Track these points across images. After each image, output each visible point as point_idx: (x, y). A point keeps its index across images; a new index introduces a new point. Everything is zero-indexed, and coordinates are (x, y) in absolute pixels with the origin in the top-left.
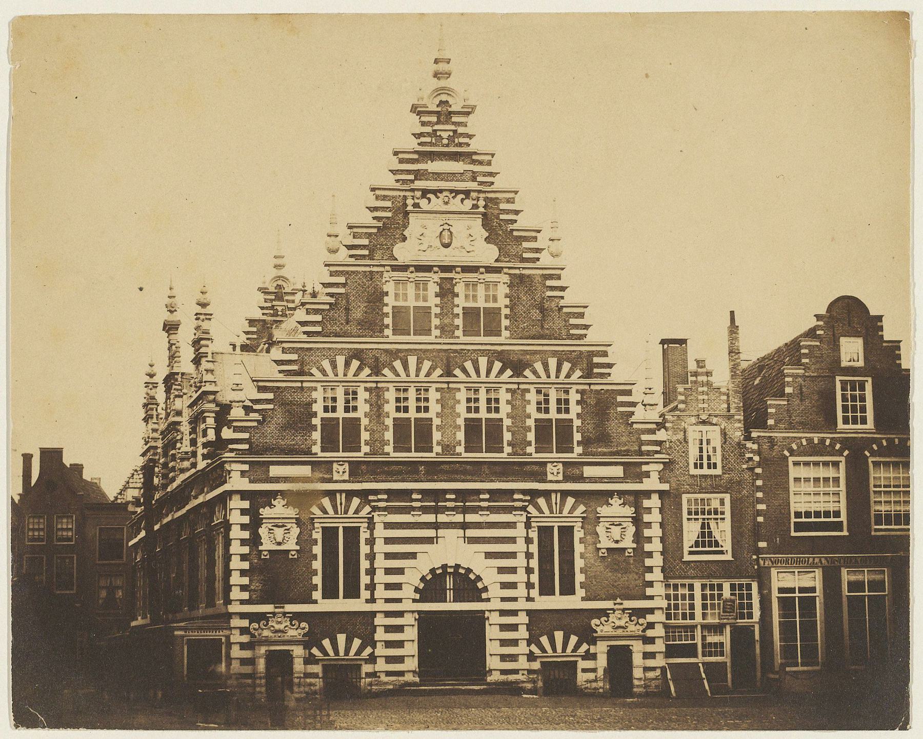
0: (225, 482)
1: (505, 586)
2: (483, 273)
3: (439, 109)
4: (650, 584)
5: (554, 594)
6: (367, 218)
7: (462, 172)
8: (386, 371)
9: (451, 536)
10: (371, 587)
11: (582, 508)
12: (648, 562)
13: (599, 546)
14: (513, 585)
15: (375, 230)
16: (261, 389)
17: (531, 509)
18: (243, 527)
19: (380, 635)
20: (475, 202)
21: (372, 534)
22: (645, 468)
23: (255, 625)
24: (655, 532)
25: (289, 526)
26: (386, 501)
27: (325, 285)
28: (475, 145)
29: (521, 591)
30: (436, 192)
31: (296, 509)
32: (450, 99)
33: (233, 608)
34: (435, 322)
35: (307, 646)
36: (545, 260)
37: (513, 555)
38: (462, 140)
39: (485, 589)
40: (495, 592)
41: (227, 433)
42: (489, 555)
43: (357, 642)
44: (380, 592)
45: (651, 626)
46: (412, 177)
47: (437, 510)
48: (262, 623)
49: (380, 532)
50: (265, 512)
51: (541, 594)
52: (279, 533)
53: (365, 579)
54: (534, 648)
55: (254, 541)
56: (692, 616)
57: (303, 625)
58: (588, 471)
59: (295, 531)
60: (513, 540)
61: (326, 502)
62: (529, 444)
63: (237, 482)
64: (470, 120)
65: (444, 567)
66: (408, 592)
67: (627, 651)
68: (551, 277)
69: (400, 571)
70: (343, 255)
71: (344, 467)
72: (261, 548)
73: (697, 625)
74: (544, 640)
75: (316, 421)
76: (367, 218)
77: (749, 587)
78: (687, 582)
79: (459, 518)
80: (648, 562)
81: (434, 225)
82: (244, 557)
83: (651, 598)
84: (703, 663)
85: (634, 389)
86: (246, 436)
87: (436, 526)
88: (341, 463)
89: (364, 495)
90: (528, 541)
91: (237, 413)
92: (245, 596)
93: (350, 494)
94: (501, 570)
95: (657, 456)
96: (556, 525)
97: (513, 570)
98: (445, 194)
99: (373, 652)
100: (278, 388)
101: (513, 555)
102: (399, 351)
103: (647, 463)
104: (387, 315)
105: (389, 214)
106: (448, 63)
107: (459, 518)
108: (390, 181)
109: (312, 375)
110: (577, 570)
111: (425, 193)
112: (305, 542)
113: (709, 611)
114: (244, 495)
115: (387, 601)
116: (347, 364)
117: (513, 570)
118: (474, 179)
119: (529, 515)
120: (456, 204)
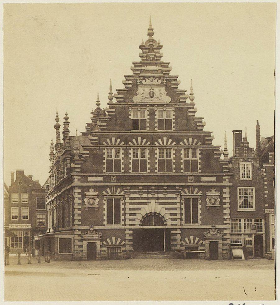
0: (73, 183)
1: (172, 220)
2: (165, 107)
3: (149, 47)
4: (225, 220)
5: (190, 223)
6: (123, 87)
7: (158, 70)
8: (130, 143)
9: (153, 202)
10: (125, 220)
11: (201, 192)
12: (225, 211)
13: (207, 206)
14: (175, 220)
15: (126, 92)
16: (85, 150)
17: (182, 192)
18: (79, 199)
20: (162, 81)
21: (125, 201)
22: (224, 178)
23: (83, 233)
24: (227, 200)
25: (95, 198)
26: (130, 189)
27: (108, 112)
29: (178, 222)
30: (148, 78)
31: (98, 193)
33: (74, 228)
34: (148, 125)
35: (102, 241)
36: (188, 101)
37: (176, 209)
38: (157, 58)
39: (165, 221)
40: (169, 222)
41: (73, 165)
42: (167, 209)
43: (119, 240)
44: (128, 222)
45: (225, 234)
47: (148, 193)
49: (128, 200)
50: (87, 193)
51: (185, 223)
53: (122, 217)
54: (183, 242)
56: (241, 231)
57: (100, 233)
58: (203, 179)
59: (97, 200)
60: (175, 203)
61: (108, 190)
62: (182, 169)
63: (76, 182)
64: (161, 51)
65: (151, 213)
66: (137, 222)
67: (217, 243)
68: (190, 108)
69: (135, 214)
70: (114, 101)
72: (85, 206)
73: (242, 234)
74: (187, 239)
75: (105, 161)
76: (123, 87)
77: (261, 220)
78: (239, 219)
79: (156, 196)
80: (225, 211)
83: (226, 224)
85: (220, 149)
87: (148, 198)
89: (123, 186)
90: (181, 204)
91: (76, 158)
92: (80, 223)
93: (117, 187)
94: (171, 214)
95: (228, 173)
96: (191, 198)
97: (175, 214)
98: (151, 78)
99: (125, 243)
100: (91, 149)
101: (176, 209)
102: (135, 135)
103: (225, 176)
105: (131, 86)
106: (153, 30)
107: (156, 196)
108: (131, 73)
109: (103, 144)
110: (199, 214)
111: (144, 78)
112: (101, 204)
113: (247, 229)
114: (79, 187)
115: (130, 225)
116: (116, 141)
117: (175, 214)
118: (162, 73)
119: (182, 195)
120: (155, 82)
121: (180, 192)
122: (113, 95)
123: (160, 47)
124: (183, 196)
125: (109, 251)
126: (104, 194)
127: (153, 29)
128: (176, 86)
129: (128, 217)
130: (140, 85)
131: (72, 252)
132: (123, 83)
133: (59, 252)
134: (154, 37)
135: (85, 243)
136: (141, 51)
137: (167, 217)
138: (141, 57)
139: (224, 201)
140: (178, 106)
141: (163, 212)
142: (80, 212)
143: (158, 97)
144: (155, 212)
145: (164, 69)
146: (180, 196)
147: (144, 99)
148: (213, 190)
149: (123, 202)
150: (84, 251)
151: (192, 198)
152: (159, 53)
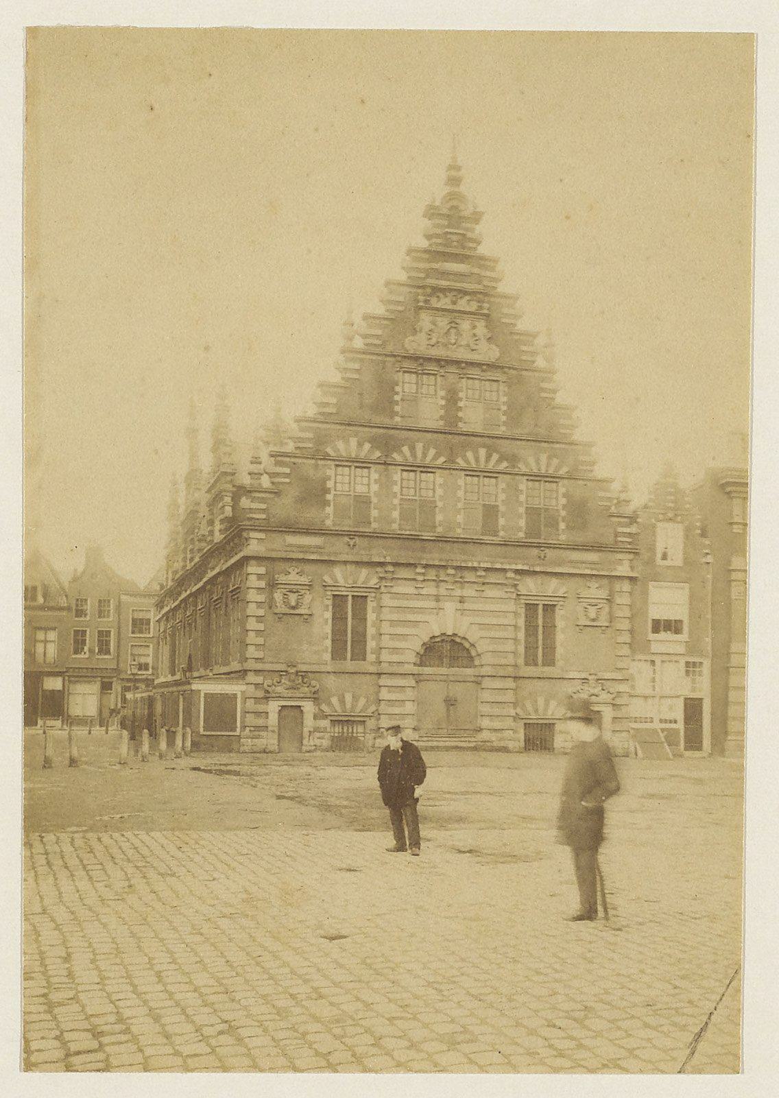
6: (380, 310)
16: (277, 463)
22: (620, 556)
28: (482, 250)
32: (462, 207)
36: (540, 363)
38: (471, 245)
40: (487, 659)
46: (422, 275)
49: (387, 600)
52: (293, 599)
53: (371, 644)
54: (519, 710)
55: (271, 604)
64: (478, 228)
66: (412, 657)
69: (404, 637)
71: (354, 540)
75: (329, 497)
79: (458, 592)
81: (443, 322)
82: (260, 619)
84: (663, 730)
86: (264, 506)
88: (352, 537)
92: (260, 655)
104: (397, 403)
107: (458, 592)
111: (436, 290)
119: (519, 593)
120: (463, 304)
121: (515, 586)
122: (355, 327)
123: (477, 217)
124: (521, 597)
125: (337, 731)
127: (459, 168)
129: (386, 641)
130: (421, 308)
131: (238, 730)
132: (382, 301)
133: (201, 730)
134: (463, 189)
135: (273, 707)
136: (427, 222)
137: (482, 646)
138: (428, 237)
140: (514, 372)
141: (473, 635)
142: (261, 627)
143: (468, 345)
144: (454, 634)
145: (483, 273)
146: (514, 596)
147: (433, 346)
148: (594, 584)
149: (375, 604)
151: (543, 603)
152: (472, 230)
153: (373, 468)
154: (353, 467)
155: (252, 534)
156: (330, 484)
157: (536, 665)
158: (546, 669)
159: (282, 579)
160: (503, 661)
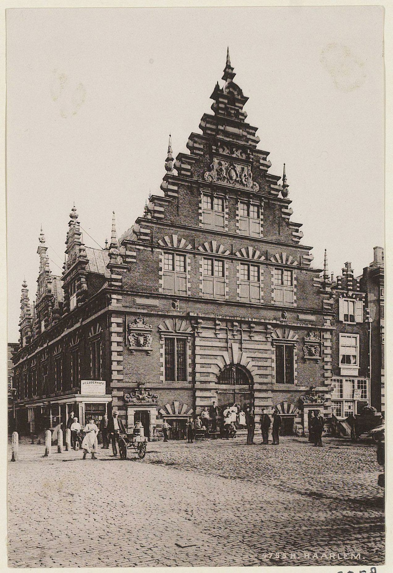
11: (297, 337)
19: (199, 402)
40: (257, 379)
48: (126, 394)
49: (198, 342)
53: (189, 370)
82: (119, 353)
86: (119, 277)
114: (118, 313)
126: (161, 329)
128: (266, 169)
137: (255, 372)
139: (326, 352)
150: (129, 426)
151: (286, 345)
153: (188, 255)
154: (175, 254)
155: (114, 296)
156: (161, 265)
157: (284, 383)
158: (289, 385)
159: (133, 326)
160: (265, 380)
